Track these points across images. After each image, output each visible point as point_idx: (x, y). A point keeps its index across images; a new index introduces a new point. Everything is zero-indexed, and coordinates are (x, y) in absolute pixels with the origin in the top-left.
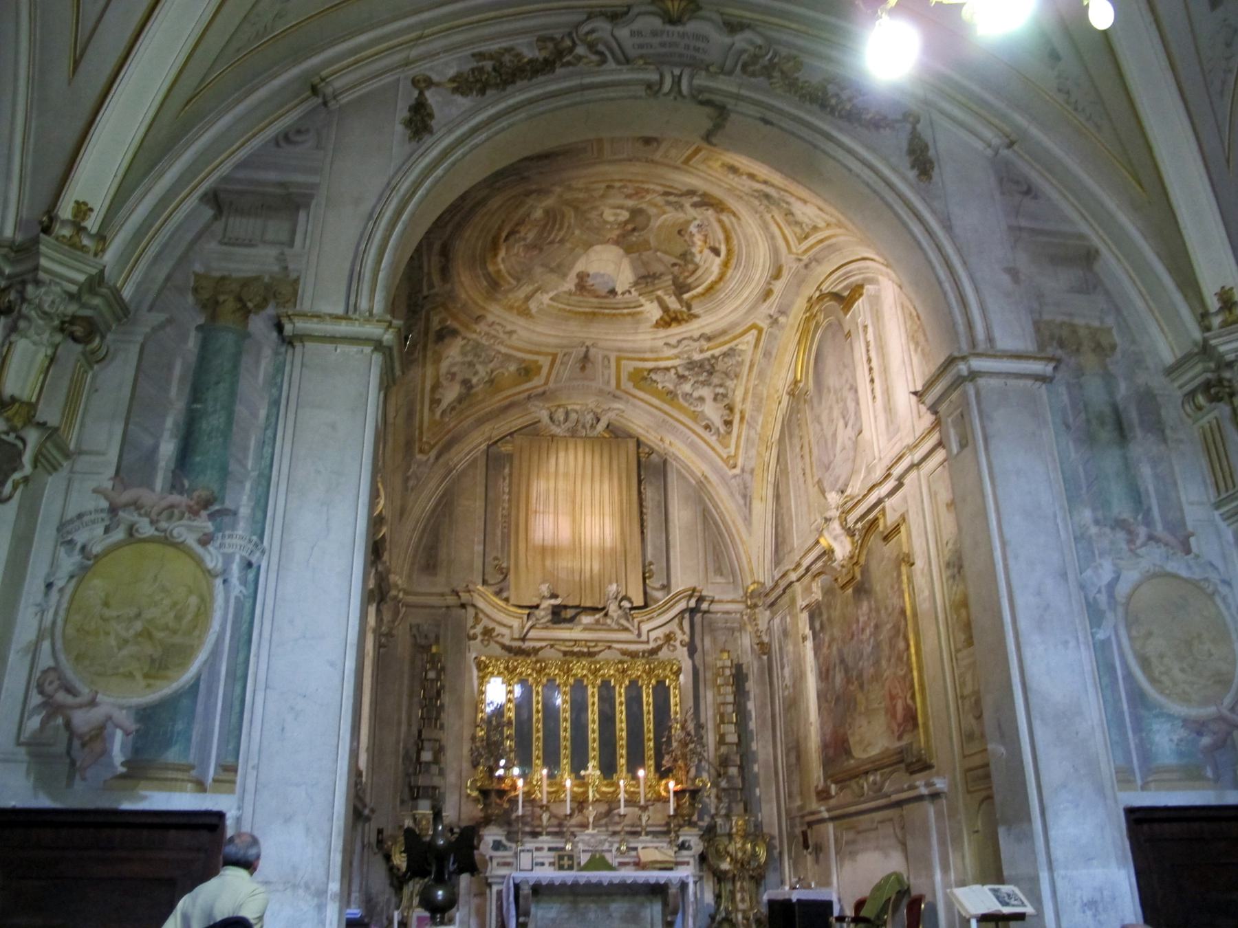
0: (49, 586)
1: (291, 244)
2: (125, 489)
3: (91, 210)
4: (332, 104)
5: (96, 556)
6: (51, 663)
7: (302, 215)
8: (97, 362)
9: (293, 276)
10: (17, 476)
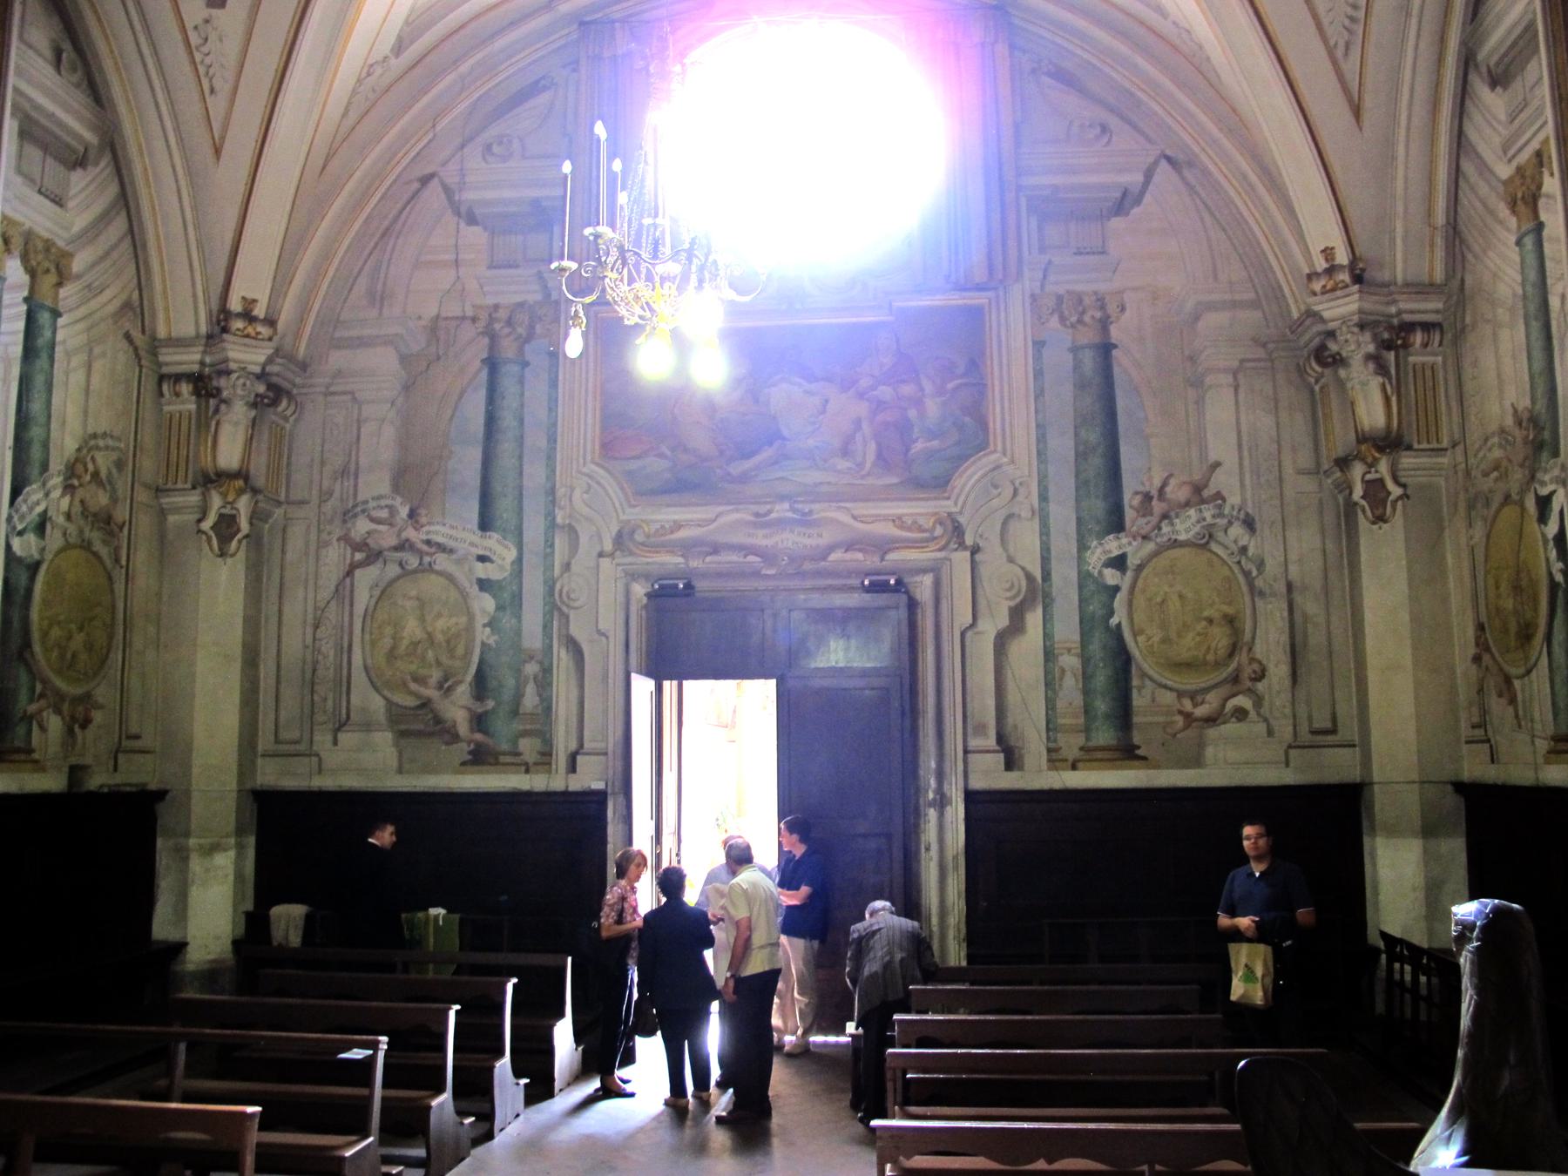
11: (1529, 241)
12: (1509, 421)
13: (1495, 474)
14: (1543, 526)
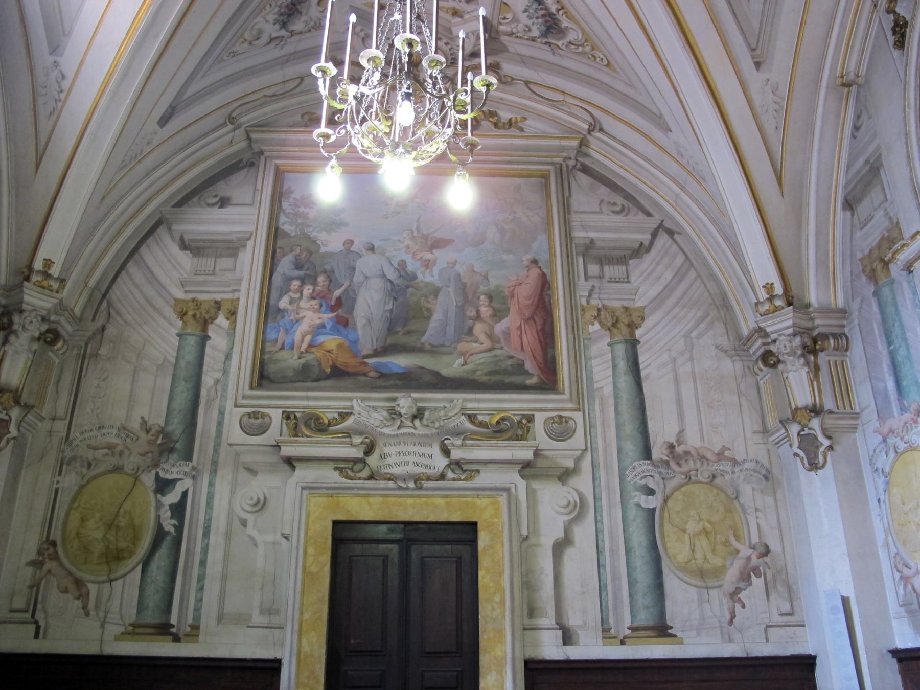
0: (879, 501)
1: (886, 199)
2: (884, 423)
3: (772, 284)
4: (860, 81)
5: (889, 473)
6: (896, 551)
7: (882, 172)
8: (847, 350)
9: (895, 221)
10: (822, 449)
11: (192, 341)
12: (135, 425)
13: (106, 451)
14: (159, 496)
